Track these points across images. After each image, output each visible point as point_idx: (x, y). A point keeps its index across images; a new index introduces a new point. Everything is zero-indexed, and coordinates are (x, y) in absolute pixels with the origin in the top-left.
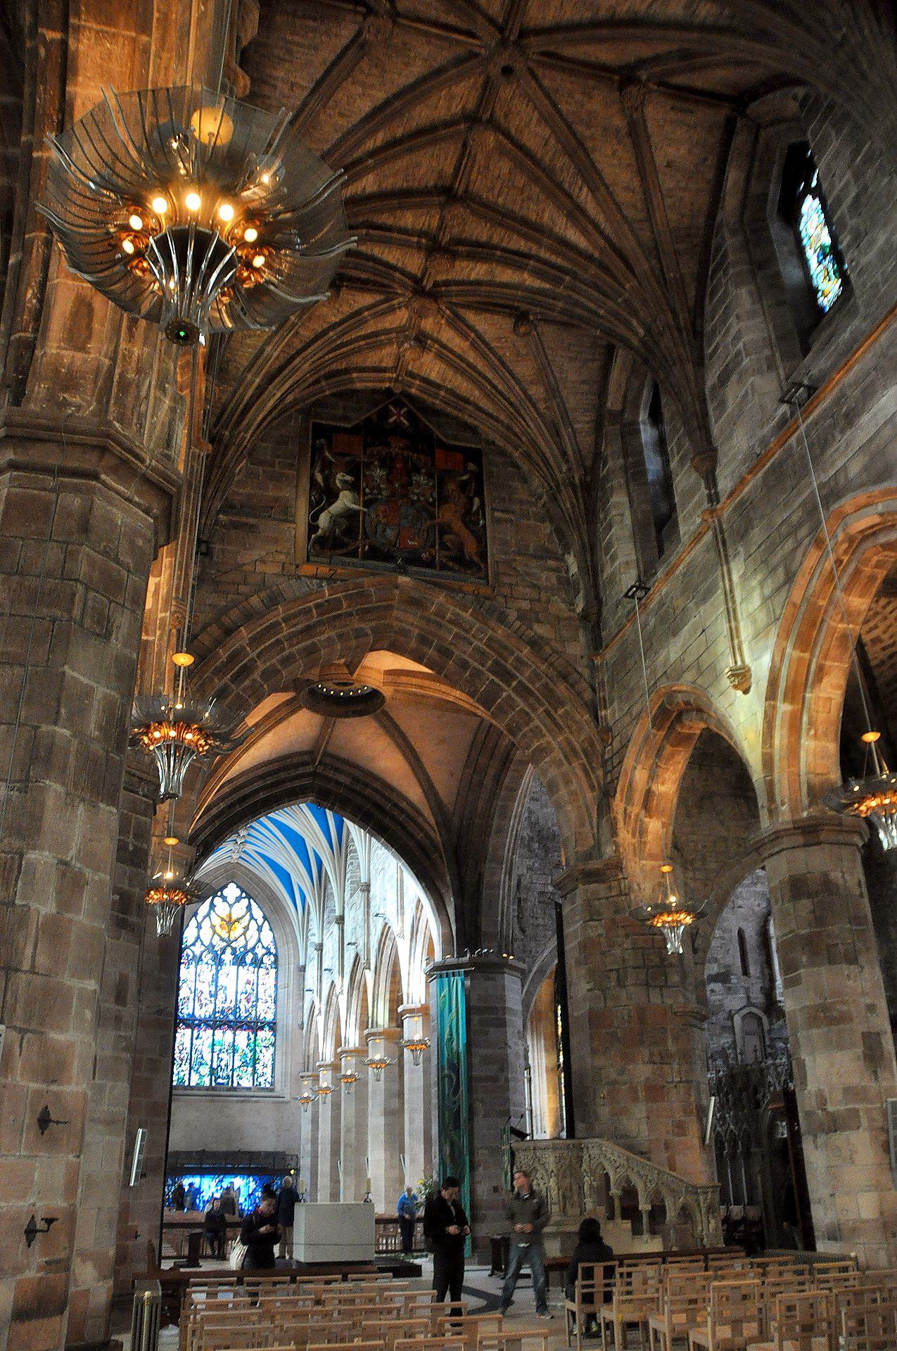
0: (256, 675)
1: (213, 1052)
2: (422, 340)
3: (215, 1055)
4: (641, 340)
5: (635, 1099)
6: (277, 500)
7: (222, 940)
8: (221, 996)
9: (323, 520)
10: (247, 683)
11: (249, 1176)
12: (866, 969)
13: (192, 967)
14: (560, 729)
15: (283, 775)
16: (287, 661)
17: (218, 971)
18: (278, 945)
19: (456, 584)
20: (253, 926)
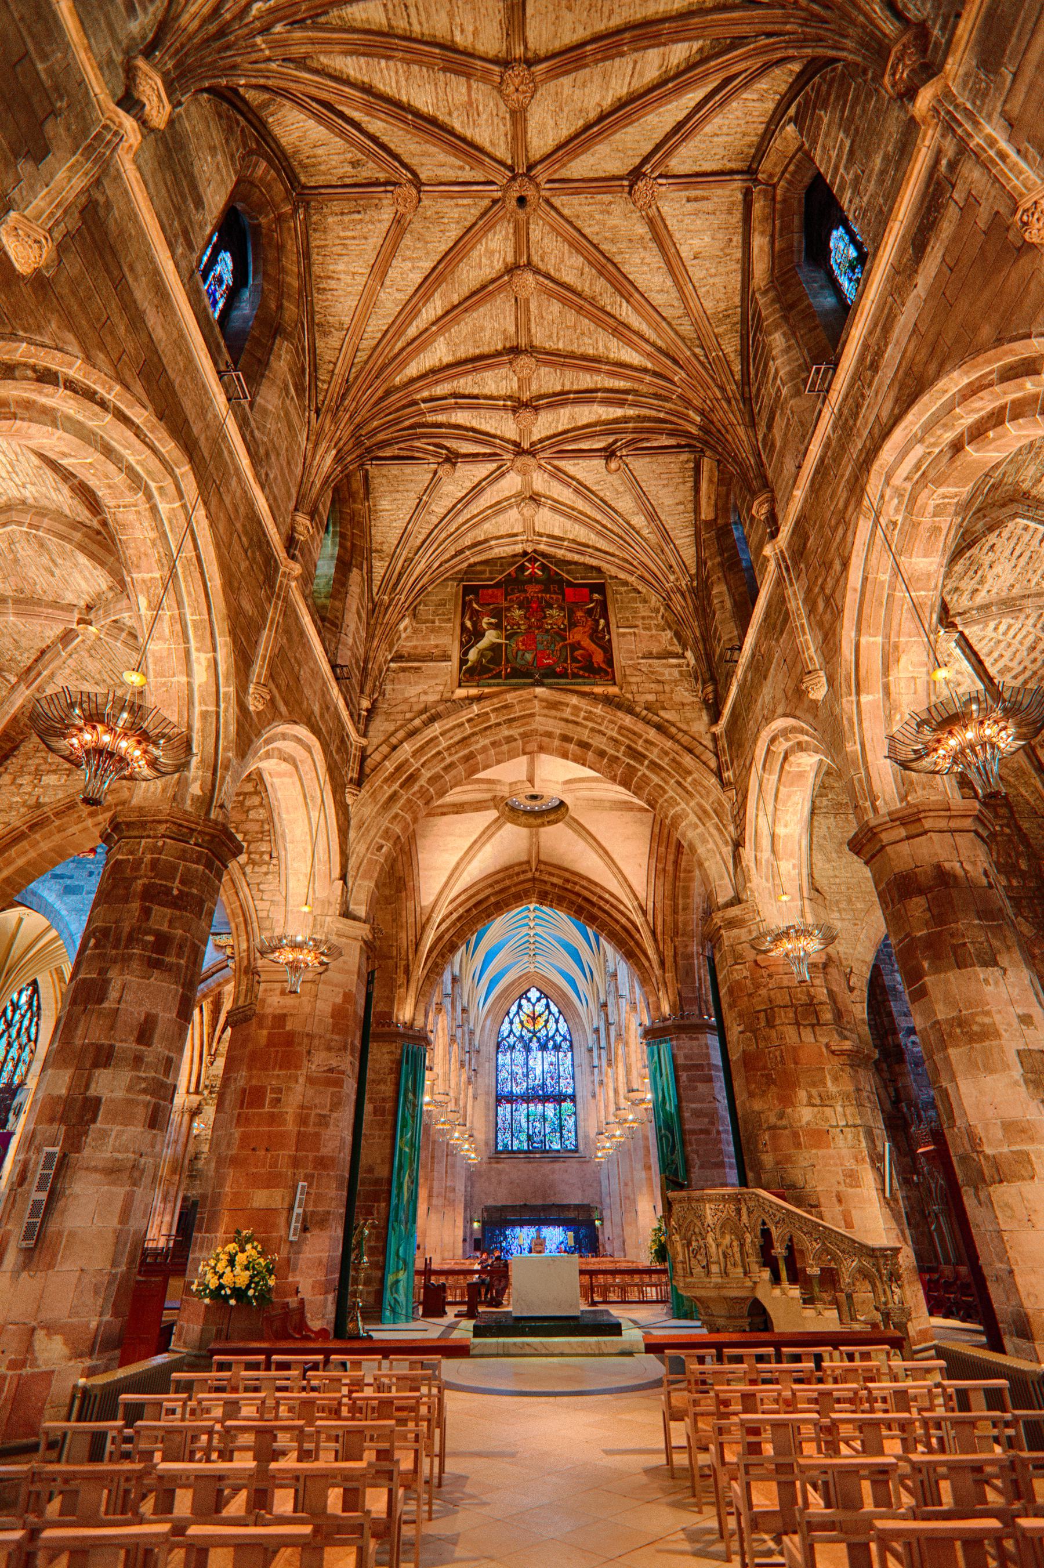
0: (422, 781)
2: (535, 499)
4: (701, 428)
5: (798, 1145)
6: (437, 646)
9: (472, 655)
10: (416, 788)
12: (1009, 973)
14: (691, 795)
15: (508, 882)
16: (447, 768)
19: (586, 689)
20: (552, 1020)
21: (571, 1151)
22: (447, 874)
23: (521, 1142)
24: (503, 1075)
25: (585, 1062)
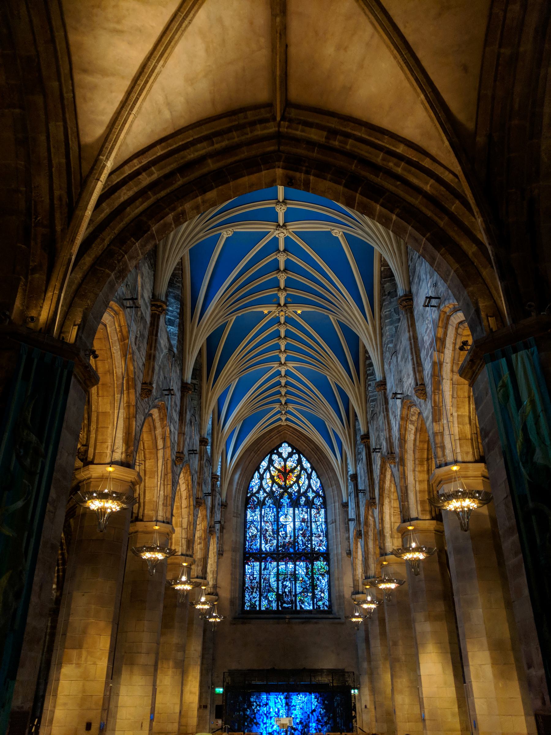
1: (278, 580)
3: (280, 582)
11: (310, 693)
13: (258, 511)
15: (236, 138)
21: (324, 612)
22: (126, 84)
23: (270, 602)
24: (253, 531)
25: (339, 519)
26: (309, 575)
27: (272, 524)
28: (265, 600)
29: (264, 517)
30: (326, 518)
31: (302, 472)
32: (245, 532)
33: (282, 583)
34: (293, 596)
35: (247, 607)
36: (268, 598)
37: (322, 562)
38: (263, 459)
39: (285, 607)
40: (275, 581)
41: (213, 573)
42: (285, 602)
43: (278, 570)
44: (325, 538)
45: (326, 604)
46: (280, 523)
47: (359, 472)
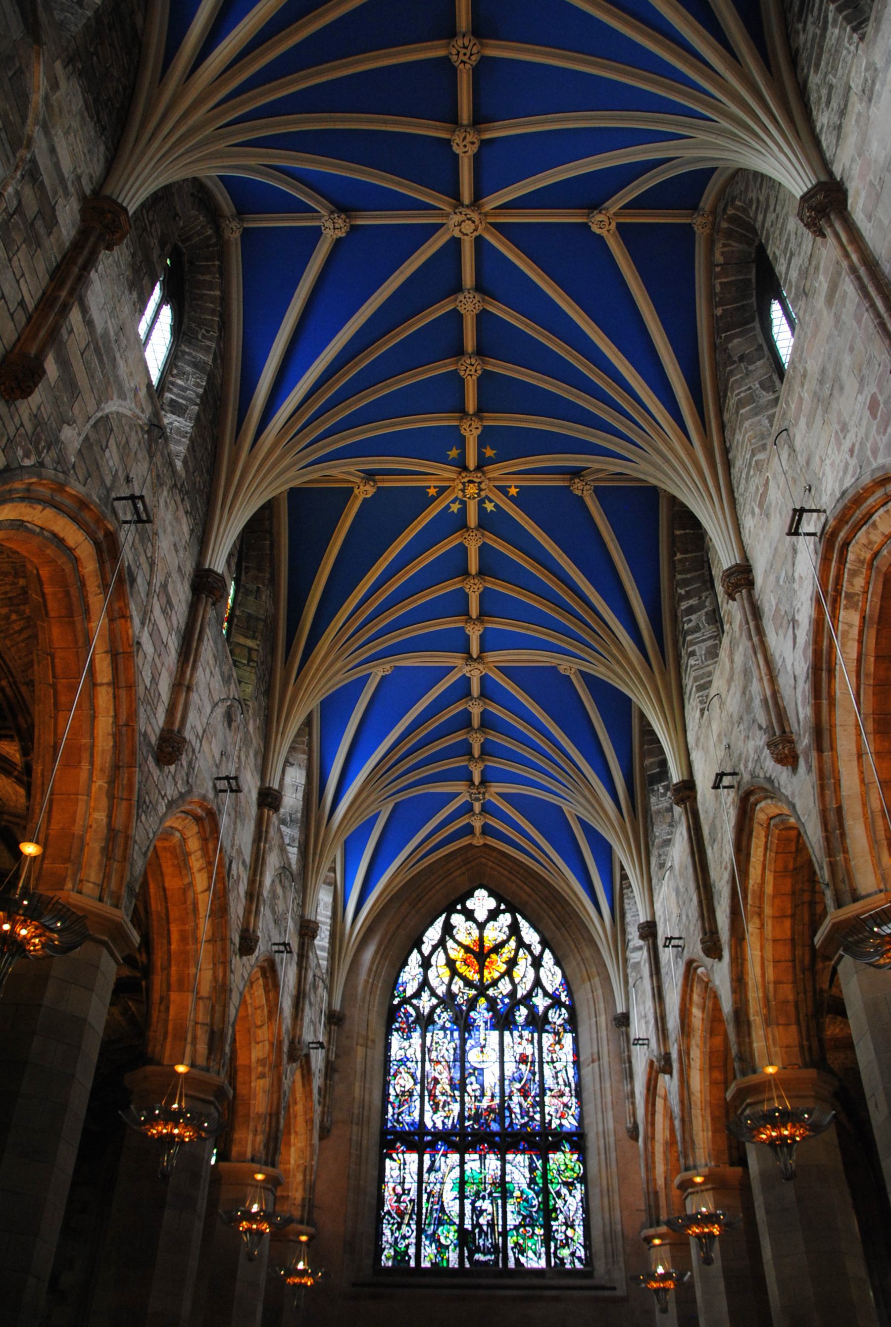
1: (462, 1197)
3: (467, 1202)
7: (468, 983)
8: (472, 1087)
13: (416, 1035)
17: (464, 1041)
18: (574, 988)
20: (524, 960)
21: (574, 1272)
23: (442, 1248)
24: (403, 1082)
26: (537, 1184)
27: (449, 1066)
28: (431, 1244)
29: (430, 1051)
30: (576, 1052)
31: (521, 950)
32: (386, 1084)
33: (473, 1203)
34: (500, 1234)
35: (388, 1259)
36: (439, 1240)
37: (568, 1155)
38: (431, 923)
39: (478, 1261)
40: (455, 1198)
41: (305, 1171)
42: (478, 1250)
43: (462, 1172)
44: (573, 1098)
45: (578, 1254)
46: (468, 1065)
47: (659, 913)
